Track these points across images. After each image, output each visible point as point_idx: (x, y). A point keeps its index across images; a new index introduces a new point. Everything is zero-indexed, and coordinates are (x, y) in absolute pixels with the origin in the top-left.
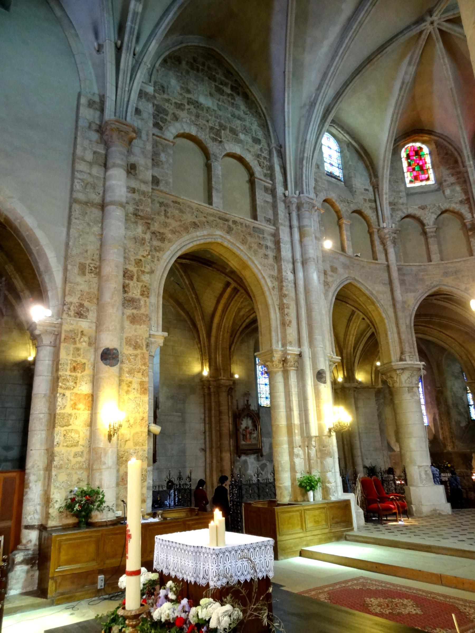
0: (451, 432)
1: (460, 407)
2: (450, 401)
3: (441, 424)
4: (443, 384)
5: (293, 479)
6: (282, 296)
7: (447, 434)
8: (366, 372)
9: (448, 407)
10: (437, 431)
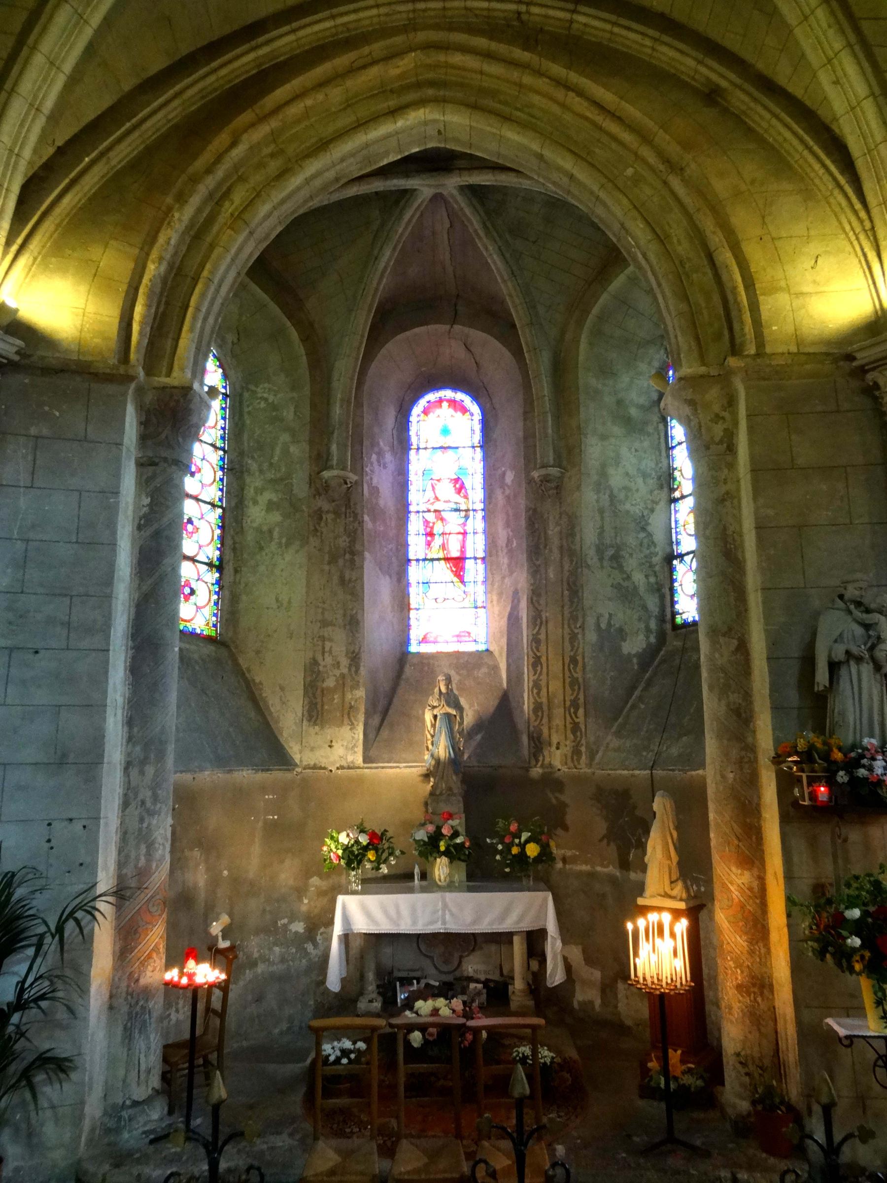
0: (574, 682)
1: (631, 563)
2: (589, 534)
3: (535, 640)
4: (568, 454)
7: (555, 686)
8: (99, 280)
9: (571, 552)
10: (515, 677)
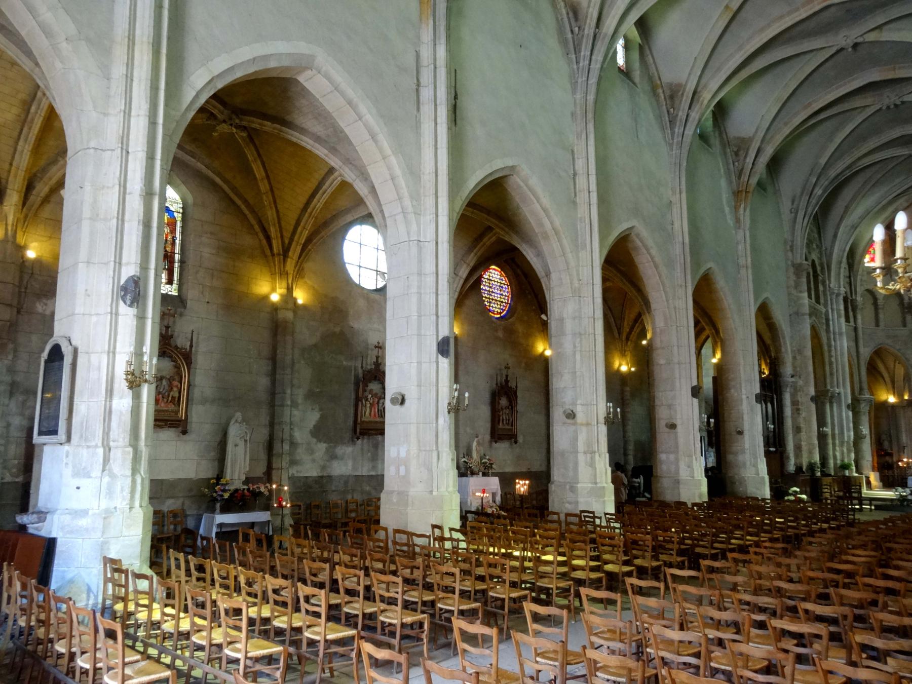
5: (835, 464)
6: (830, 356)
